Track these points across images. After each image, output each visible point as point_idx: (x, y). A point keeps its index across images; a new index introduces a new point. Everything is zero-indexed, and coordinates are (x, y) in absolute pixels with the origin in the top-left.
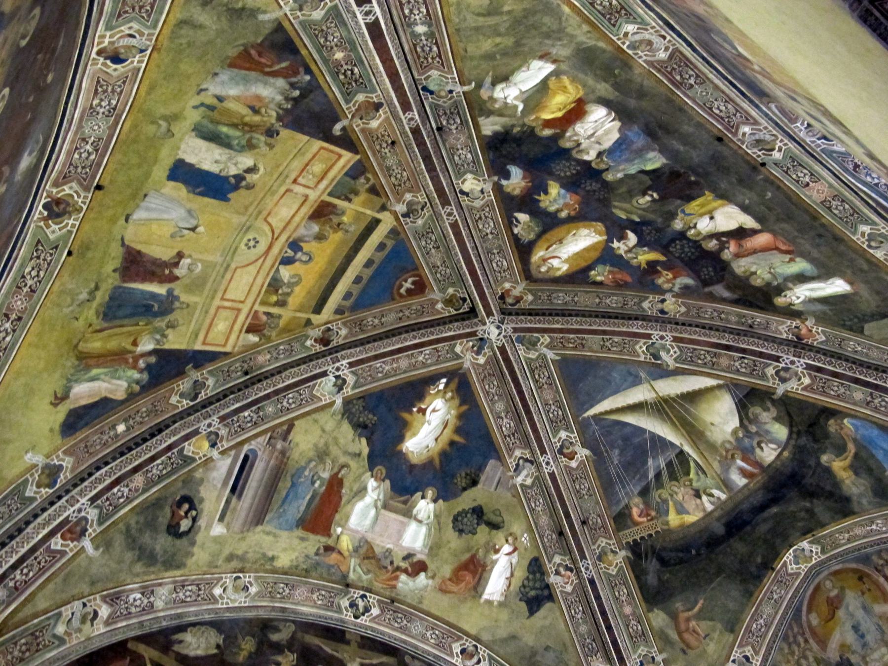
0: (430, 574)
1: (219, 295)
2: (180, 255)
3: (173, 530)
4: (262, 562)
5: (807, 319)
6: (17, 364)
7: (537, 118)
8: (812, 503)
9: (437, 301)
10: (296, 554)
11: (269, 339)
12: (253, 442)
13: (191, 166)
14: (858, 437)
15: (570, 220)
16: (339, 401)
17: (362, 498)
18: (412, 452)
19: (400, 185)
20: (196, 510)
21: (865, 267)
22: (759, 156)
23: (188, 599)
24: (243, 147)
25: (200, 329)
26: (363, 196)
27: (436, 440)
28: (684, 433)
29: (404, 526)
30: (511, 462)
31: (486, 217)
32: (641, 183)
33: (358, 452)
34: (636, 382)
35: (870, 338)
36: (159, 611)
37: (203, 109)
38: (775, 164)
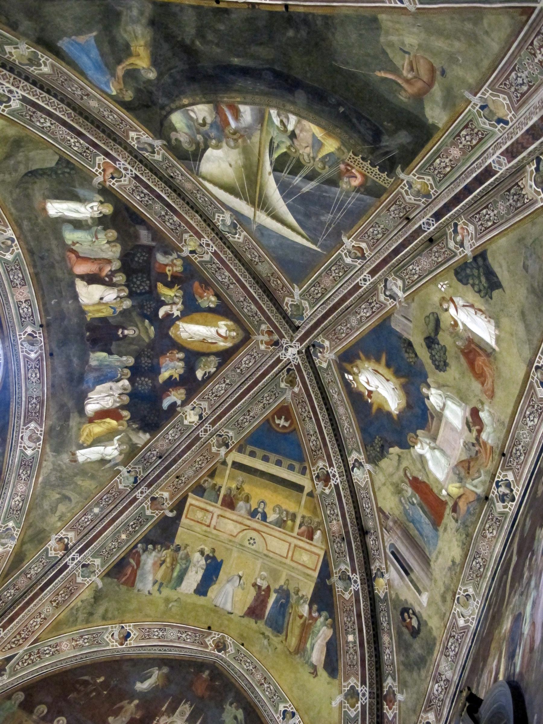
0: (479, 406)
1: (284, 560)
2: (254, 585)
3: (415, 633)
4: (454, 572)
5: (99, 183)
6: (285, 688)
7: (119, 425)
8: (193, 42)
9: (293, 392)
10: (454, 539)
11: (320, 523)
12: (386, 544)
13: (198, 585)
14: (108, 77)
15: (180, 348)
16: (368, 467)
17: (427, 461)
18: (398, 404)
19: (207, 459)
20: (409, 609)
21: (25, 223)
22: (40, 333)
23: (457, 650)
24: (187, 561)
25: (304, 573)
26: (217, 480)
27: (388, 380)
28: (259, 177)
29: (448, 423)
30: (390, 304)
31: (213, 393)
32: (119, 346)
33: (397, 458)
34: (262, 228)
35: (57, 152)
36: (453, 677)
37: (161, 589)
38: (34, 324)
